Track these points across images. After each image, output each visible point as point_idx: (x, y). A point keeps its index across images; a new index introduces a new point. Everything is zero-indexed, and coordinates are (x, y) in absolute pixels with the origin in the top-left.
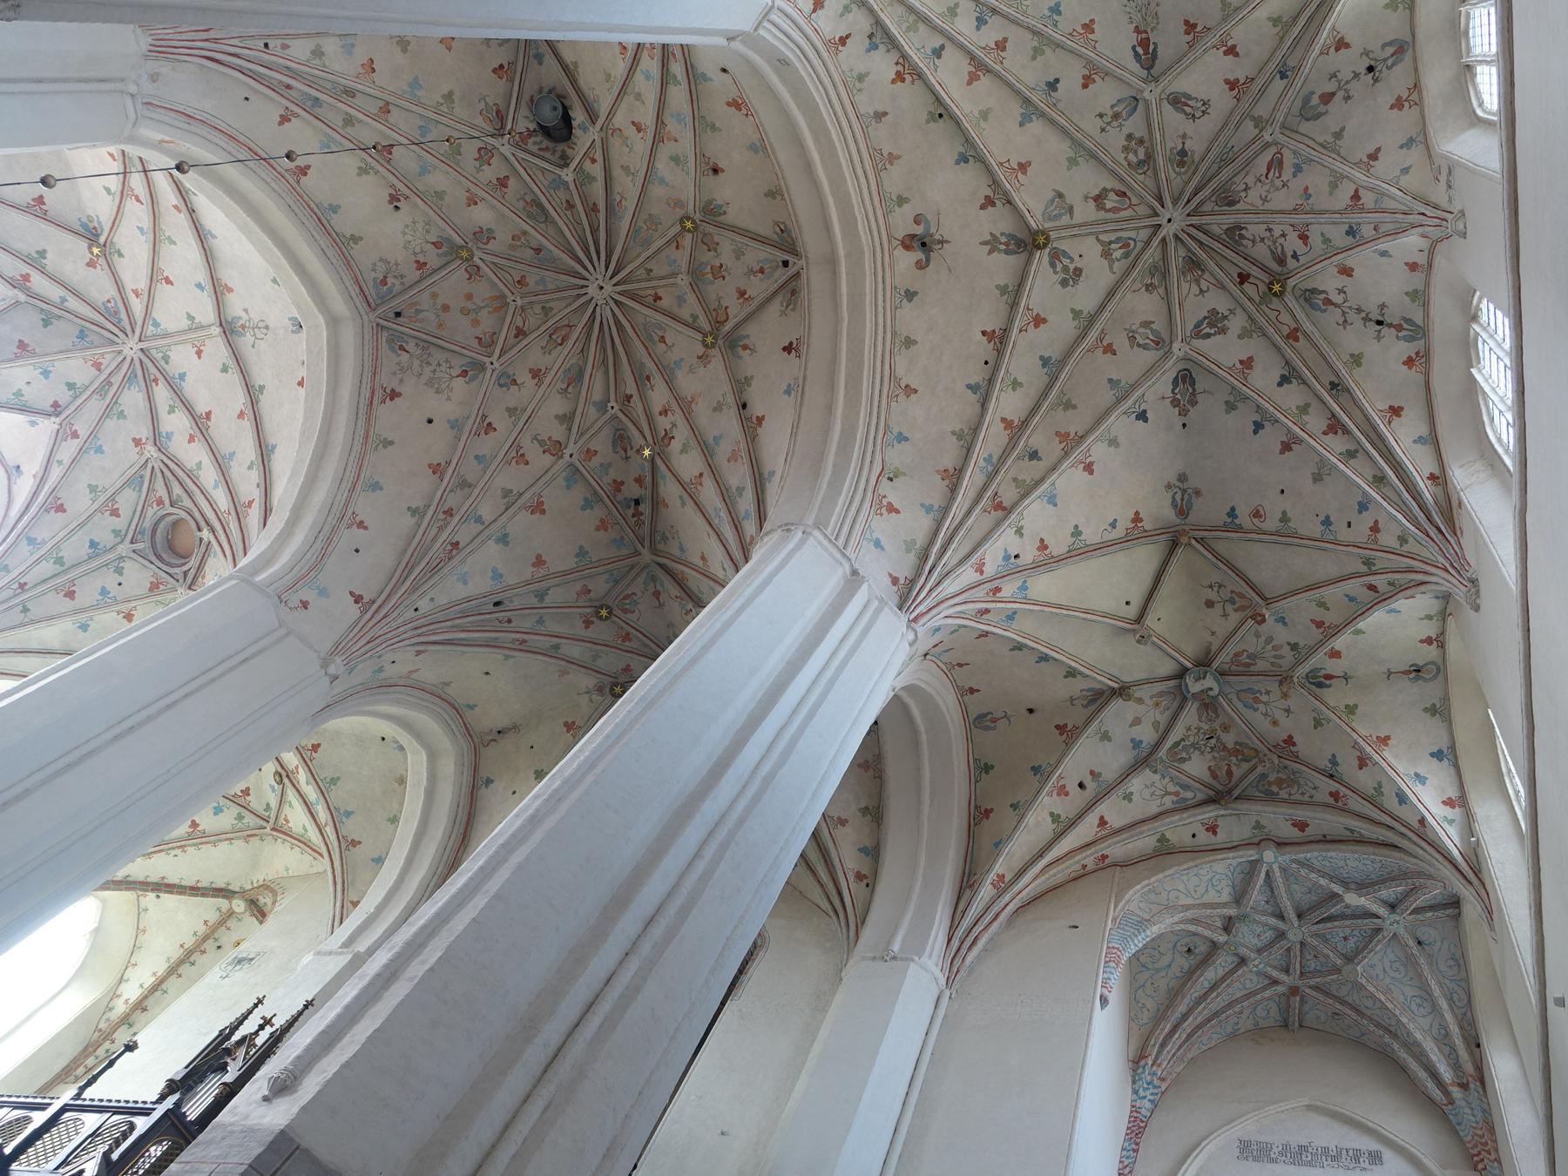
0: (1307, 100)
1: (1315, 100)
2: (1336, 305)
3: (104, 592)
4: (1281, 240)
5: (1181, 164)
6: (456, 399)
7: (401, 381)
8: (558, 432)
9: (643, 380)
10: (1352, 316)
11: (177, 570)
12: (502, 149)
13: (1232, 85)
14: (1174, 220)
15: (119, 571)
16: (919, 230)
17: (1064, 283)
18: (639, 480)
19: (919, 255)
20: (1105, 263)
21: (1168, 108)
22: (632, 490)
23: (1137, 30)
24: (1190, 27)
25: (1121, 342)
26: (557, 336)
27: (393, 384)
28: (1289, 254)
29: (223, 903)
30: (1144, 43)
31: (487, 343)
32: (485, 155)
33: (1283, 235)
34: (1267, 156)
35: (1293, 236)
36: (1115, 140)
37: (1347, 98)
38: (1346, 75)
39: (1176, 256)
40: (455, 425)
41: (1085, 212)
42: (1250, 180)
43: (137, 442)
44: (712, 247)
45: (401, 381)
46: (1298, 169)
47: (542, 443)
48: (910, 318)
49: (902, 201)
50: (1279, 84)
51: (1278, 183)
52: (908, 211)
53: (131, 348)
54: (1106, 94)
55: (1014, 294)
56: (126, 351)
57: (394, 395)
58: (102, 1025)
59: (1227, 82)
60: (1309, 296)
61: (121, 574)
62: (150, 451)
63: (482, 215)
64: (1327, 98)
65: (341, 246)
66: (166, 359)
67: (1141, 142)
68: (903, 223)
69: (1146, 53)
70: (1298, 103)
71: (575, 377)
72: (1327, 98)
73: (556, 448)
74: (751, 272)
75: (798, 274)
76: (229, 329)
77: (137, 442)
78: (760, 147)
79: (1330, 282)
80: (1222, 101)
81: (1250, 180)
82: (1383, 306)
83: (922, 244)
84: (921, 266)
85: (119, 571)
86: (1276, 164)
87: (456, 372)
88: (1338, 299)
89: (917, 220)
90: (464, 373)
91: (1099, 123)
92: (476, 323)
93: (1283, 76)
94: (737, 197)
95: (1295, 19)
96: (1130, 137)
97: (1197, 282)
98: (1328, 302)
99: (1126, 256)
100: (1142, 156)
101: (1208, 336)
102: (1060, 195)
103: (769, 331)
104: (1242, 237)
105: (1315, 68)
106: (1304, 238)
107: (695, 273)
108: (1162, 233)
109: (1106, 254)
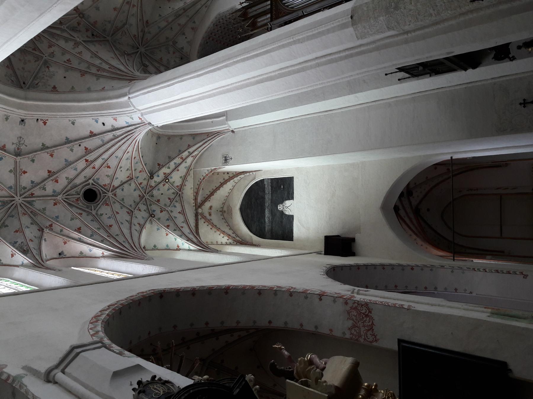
3: (109, 218)
7: (49, 85)
11: (102, 195)
15: (102, 215)
22: (89, 34)
29: (200, 217)
40: (67, 71)
43: (55, 204)
45: (49, 85)
47: (74, 48)
53: (18, 200)
56: (20, 201)
58: (235, 243)
61: (103, 214)
62: (59, 198)
66: (25, 188)
73: (77, 44)
76: (18, 153)
77: (55, 204)
85: (102, 215)
87: (47, 70)
90: (48, 67)
92: (29, 61)
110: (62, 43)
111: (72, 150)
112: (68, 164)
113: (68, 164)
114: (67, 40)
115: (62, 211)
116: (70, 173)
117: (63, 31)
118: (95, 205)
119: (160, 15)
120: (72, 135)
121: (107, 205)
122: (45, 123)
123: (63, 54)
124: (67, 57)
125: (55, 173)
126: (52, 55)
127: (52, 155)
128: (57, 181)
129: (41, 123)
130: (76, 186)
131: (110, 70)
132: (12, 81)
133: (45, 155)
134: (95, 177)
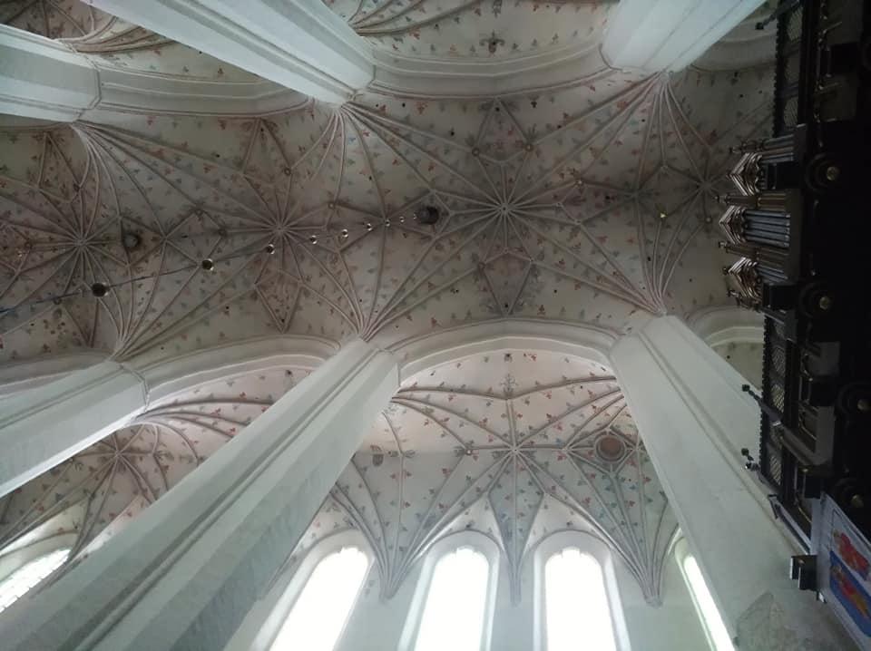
3: (633, 488)
6: (547, 280)
8: (568, 230)
9: (547, 187)
12: (438, 237)
15: (623, 480)
16: (487, 44)
18: (596, 195)
19: (498, 44)
22: (601, 199)
26: (525, 231)
27: (537, 310)
31: (523, 263)
32: (439, 247)
40: (558, 280)
43: (560, 458)
44: (489, 146)
47: (571, 237)
48: (524, 45)
49: (473, 49)
52: (477, 47)
53: (515, 450)
56: (517, 452)
57: (542, 309)
62: (564, 451)
63: (466, 255)
65: (470, 318)
66: (522, 435)
68: (485, 50)
71: (543, 222)
73: (575, 230)
74: (501, 128)
75: (503, 102)
76: (509, 395)
77: (560, 458)
78: (443, 103)
83: (493, 43)
84: (503, 43)
85: (623, 480)
87: (534, 280)
89: (482, 44)
94: (467, 125)
103: (528, 117)
107: (500, 157)
110: (556, 231)
111: (573, 392)
112: (572, 409)
113: (572, 409)
114: (562, 226)
115: (566, 468)
116: (575, 419)
117: (558, 209)
118: (615, 462)
119: (739, 114)
120: (570, 375)
121: (633, 464)
122: (534, 358)
123: (555, 252)
124: (560, 257)
125: (556, 419)
126: (542, 256)
127: (549, 396)
128: (560, 428)
129: (529, 357)
130: (587, 435)
131: (613, 279)
132: (490, 308)
133: (540, 395)
134: (615, 423)
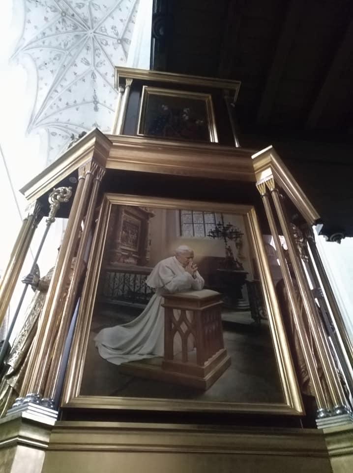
0: (59, 59)
1: (58, 58)
2: (48, 7)
4: (63, 27)
5: (88, 47)
10: (44, 4)
13: (76, 65)
14: (90, 33)
17: (115, 27)
20: (106, 28)
21: (90, 62)
23: (95, 81)
24: (84, 80)
25: (102, 7)
28: (61, 23)
30: (94, 78)
33: (62, 28)
34: (68, 47)
35: (60, 29)
36: (103, 57)
37: (50, 59)
38: (51, 63)
39: (89, 24)
41: (110, 41)
42: (72, 41)
46: (60, 44)
50: (66, 64)
51: (65, 41)
54: (102, 69)
55: (127, 29)
59: (77, 66)
60: (55, 11)
64: (55, 59)
67: (97, 55)
69: (93, 76)
70: (61, 58)
72: (55, 59)
79: (51, 15)
80: (78, 61)
81: (72, 41)
82: (36, 7)
86: (65, 45)
88: (49, 9)
91: (105, 63)
93: (64, 66)
95: (62, 79)
96: (99, 57)
97: (85, 17)
98: (51, 8)
99: (101, 28)
100: (97, 51)
101: (81, 3)
102: (115, 49)
104: (74, 27)
105: (57, 66)
106: (57, 29)
108: (93, 30)
109: (106, 30)
